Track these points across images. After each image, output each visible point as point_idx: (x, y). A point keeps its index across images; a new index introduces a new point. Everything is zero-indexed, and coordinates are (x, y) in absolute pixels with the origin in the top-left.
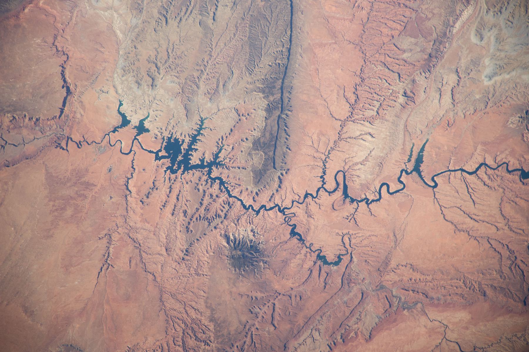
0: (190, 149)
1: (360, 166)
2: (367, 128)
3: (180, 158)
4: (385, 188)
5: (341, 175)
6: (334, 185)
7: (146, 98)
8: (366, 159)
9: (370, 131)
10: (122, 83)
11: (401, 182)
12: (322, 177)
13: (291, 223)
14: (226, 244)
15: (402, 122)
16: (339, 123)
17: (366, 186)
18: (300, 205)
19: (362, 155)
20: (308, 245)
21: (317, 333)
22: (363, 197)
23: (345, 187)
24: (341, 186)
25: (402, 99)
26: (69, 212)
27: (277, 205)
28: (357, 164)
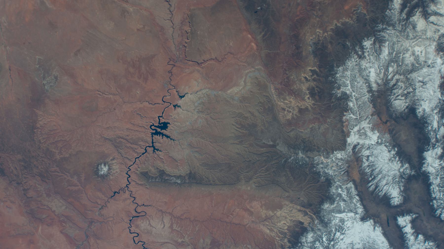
0: (163, 135)
1: (148, 223)
2: (167, 225)
3: (159, 130)
4: (136, 235)
5: (144, 214)
6: (139, 211)
7: (193, 108)
8: (151, 226)
9: (166, 227)
10: (202, 94)
11: (138, 242)
12: (143, 205)
13: (120, 191)
14: (110, 159)
15: (169, 241)
16: (171, 212)
17: (137, 226)
18: (129, 195)
19: (153, 223)
20: (109, 200)
21: (64, 208)
22: (132, 225)
23: (138, 217)
24: (138, 215)
25: (180, 240)
26: (131, 70)
27: (130, 183)
28: (149, 222)
